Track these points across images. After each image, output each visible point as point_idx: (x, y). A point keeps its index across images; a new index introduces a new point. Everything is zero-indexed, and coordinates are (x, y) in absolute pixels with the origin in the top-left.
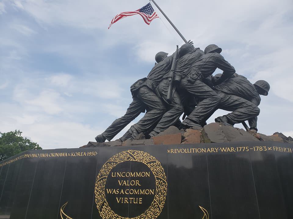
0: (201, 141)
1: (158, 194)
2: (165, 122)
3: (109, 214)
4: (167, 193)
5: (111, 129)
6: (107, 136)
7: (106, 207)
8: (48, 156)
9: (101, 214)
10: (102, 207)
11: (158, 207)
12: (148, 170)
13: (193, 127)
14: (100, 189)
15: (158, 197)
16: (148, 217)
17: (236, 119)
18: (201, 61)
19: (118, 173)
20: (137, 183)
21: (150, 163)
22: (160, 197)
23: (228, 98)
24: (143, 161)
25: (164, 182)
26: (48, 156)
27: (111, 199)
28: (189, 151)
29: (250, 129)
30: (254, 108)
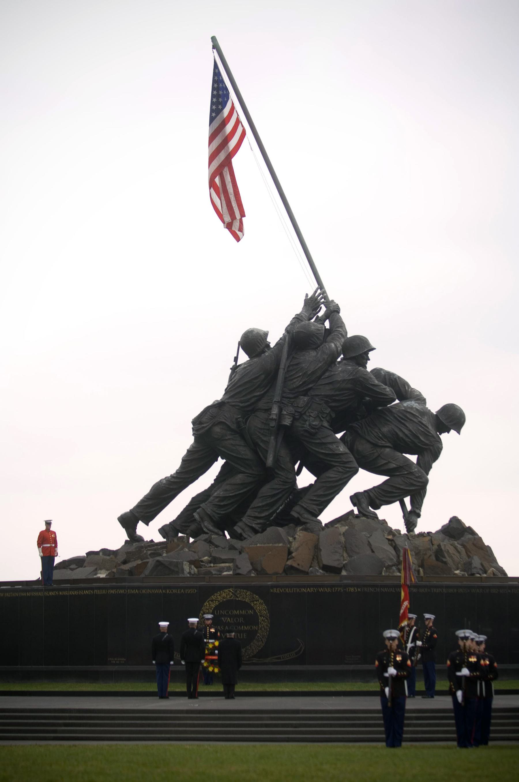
0: (314, 558)
1: (261, 629)
2: (263, 506)
5: (150, 503)
11: (262, 640)
12: (252, 608)
13: (308, 525)
20: (241, 620)
21: (253, 601)
23: (376, 454)
28: (291, 590)
29: (410, 511)
30: (417, 477)
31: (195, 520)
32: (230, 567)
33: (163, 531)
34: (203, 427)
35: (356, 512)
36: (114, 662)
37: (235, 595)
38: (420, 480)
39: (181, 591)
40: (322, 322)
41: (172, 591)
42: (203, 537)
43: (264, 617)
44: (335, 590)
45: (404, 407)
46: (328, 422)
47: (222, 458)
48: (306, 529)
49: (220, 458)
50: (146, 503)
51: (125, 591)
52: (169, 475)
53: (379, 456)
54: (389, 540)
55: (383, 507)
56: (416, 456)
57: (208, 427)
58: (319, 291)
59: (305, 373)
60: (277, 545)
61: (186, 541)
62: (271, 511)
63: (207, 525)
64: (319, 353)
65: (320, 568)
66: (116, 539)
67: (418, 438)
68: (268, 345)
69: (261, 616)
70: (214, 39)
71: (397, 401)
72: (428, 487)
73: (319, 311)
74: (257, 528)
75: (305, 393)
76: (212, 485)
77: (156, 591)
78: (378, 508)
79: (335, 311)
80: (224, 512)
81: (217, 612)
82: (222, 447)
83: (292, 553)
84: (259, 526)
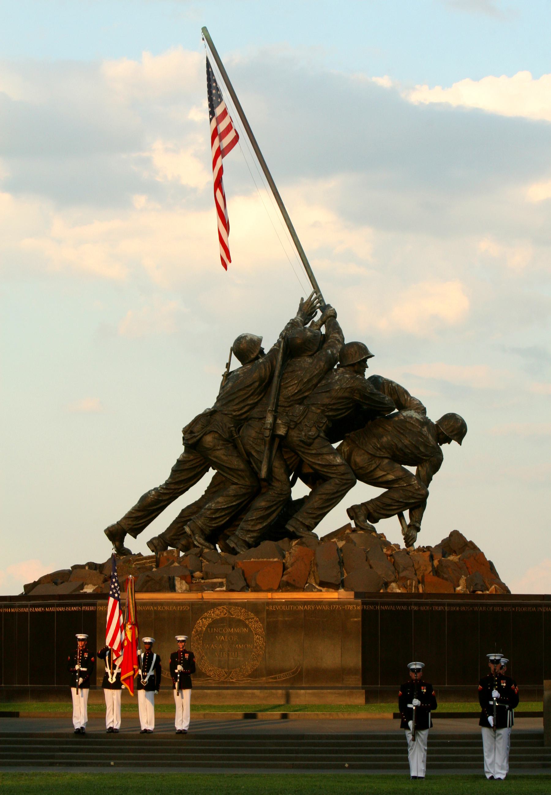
2: (257, 519)
6: (130, 529)
11: (257, 659)
12: (246, 626)
13: (304, 540)
17: (383, 512)
18: (328, 394)
21: (248, 619)
23: (374, 466)
29: (409, 526)
30: (416, 490)
31: (185, 532)
32: (222, 582)
33: (151, 544)
34: (195, 437)
35: (353, 526)
37: (229, 612)
38: (421, 493)
40: (318, 328)
41: (164, 608)
42: (194, 551)
44: (333, 607)
45: (404, 416)
46: (325, 432)
47: (214, 469)
48: (301, 544)
49: (211, 469)
50: (134, 515)
52: (158, 486)
53: (377, 467)
54: (388, 555)
55: (381, 521)
56: (416, 467)
57: (199, 437)
58: (315, 295)
59: (300, 381)
60: (271, 560)
61: (176, 555)
62: (265, 524)
63: (198, 540)
64: (316, 360)
65: (316, 584)
66: (103, 552)
67: (419, 449)
68: (262, 351)
69: (256, 634)
70: (205, 30)
71: (396, 411)
72: (428, 500)
73: (315, 316)
74: (250, 542)
75: (301, 402)
76: (203, 496)
77: (148, 608)
78: (376, 521)
79: (331, 316)
80: (216, 525)
82: (214, 457)
83: (288, 568)
84: (252, 540)
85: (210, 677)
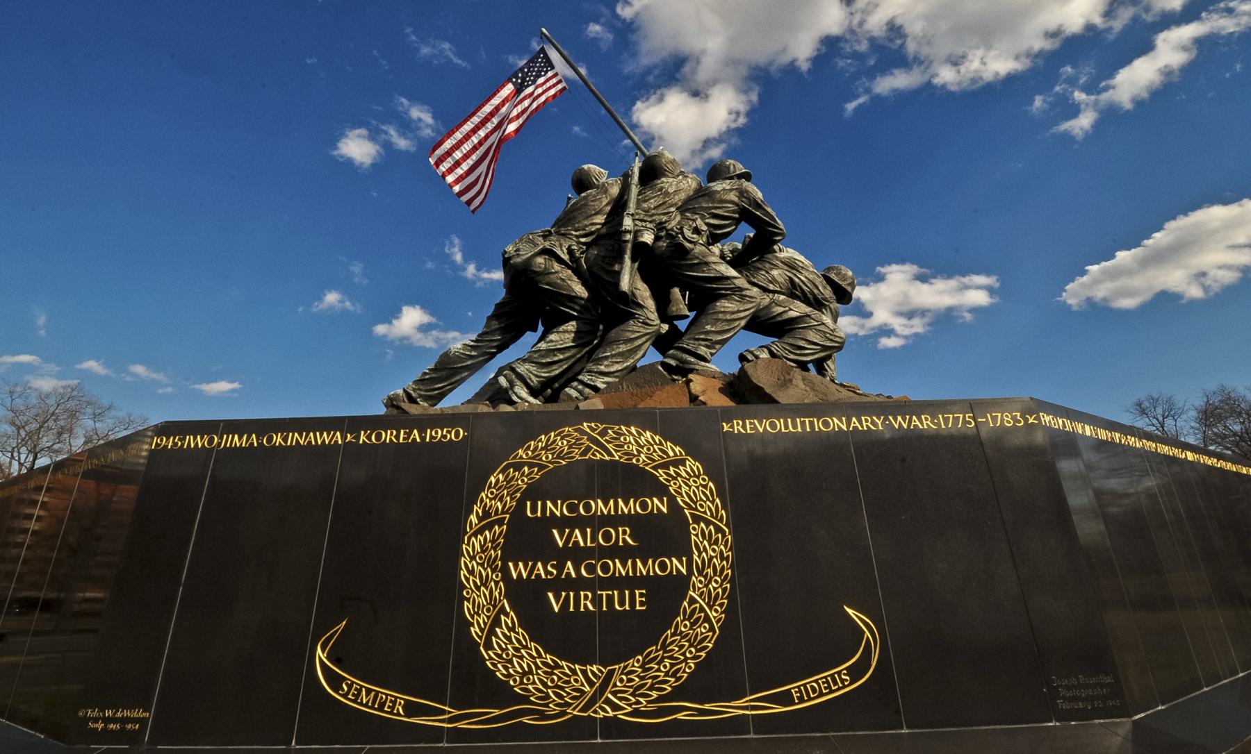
1: (700, 573)
3: (521, 657)
4: (732, 567)
7: (510, 629)
8: (260, 444)
9: (491, 658)
10: (492, 632)
11: (707, 619)
12: (661, 490)
14: (482, 565)
15: (700, 582)
16: (671, 658)
17: (792, 357)
19: (549, 504)
20: (624, 536)
21: (665, 466)
22: (710, 582)
24: (638, 460)
25: (718, 529)
26: (260, 444)
27: (526, 598)
28: (795, 426)
36: (100, 726)
39: (409, 434)
41: (379, 437)
43: (708, 523)
51: (211, 441)
69: (697, 519)
81: (534, 510)
85: (525, 700)
